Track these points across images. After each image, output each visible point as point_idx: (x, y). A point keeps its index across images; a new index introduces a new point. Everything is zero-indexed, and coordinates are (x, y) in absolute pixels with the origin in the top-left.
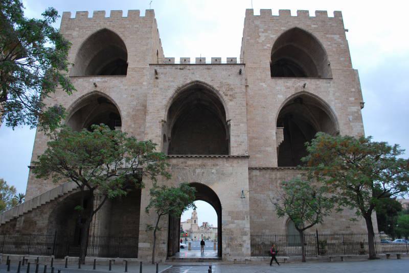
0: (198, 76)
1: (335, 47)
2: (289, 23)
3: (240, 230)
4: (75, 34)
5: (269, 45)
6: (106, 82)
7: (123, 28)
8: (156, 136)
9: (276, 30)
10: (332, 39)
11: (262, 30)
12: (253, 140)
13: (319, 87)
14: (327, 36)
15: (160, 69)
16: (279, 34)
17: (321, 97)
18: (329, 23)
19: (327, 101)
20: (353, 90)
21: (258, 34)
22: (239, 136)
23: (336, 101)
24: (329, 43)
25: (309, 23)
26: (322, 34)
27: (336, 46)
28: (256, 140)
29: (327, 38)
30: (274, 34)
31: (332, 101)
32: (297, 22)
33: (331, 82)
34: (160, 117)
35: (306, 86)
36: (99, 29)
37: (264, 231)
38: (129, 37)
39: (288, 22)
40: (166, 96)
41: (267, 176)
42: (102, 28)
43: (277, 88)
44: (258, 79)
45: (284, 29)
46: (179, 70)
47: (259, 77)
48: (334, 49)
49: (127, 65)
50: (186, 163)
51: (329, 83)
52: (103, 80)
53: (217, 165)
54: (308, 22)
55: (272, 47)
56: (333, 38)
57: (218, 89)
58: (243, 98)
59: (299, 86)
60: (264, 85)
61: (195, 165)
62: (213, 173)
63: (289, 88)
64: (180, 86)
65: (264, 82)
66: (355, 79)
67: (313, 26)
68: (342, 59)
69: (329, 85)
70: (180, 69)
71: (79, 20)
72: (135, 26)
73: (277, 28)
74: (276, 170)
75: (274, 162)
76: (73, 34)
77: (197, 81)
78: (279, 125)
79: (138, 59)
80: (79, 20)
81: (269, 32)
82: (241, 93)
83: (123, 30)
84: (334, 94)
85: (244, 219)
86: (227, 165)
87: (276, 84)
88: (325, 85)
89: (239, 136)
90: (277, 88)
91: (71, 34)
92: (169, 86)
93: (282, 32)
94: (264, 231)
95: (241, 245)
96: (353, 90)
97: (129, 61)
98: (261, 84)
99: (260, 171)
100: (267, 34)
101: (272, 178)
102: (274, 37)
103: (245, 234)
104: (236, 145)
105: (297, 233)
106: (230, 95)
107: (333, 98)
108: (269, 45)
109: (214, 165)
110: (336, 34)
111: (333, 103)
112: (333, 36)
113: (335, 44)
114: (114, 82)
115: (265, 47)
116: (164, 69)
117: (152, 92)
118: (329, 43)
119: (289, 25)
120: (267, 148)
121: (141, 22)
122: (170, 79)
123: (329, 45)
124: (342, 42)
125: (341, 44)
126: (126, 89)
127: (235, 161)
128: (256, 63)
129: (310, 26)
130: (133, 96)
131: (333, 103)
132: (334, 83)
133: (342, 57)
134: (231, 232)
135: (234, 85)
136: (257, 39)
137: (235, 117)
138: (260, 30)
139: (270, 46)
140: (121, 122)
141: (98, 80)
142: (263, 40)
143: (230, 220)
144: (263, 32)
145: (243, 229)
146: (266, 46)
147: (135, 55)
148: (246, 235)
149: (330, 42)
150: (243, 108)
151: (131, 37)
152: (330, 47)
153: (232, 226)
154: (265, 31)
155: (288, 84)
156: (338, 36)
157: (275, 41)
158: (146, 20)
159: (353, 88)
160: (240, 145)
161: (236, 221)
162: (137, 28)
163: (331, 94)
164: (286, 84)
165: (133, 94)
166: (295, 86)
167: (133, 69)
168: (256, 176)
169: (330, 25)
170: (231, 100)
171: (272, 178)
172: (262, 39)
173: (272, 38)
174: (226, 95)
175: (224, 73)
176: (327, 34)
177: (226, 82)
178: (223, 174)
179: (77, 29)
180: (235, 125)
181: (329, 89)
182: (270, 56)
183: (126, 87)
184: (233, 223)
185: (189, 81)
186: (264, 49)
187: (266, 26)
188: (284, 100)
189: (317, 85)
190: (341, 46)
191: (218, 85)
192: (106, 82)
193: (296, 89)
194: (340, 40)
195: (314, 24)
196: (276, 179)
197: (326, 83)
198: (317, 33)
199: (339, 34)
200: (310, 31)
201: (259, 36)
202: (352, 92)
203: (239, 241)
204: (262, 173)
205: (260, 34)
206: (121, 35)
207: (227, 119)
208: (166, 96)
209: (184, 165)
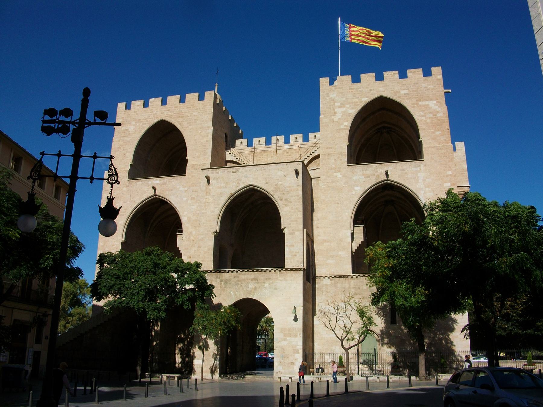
0: (251, 179)
1: (430, 118)
2: (372, 92)
3: (293, 347)
4: (131, 128)
5: (346, 124)
6: (165, 184)
7: (182, 117)
8: (209, 250)
9: (354, 102)
10: (427, 106)
11: (339, 104)
12: (325, 244)
13: (406, 173)
14: (420, 103)
15: (213, 173)
16: (359, 108)
17: (407, 185)
18: (424, 85)
19: (414, 190)
20: (450, 173)
21: (334, 110)
22: (293, 246)
23: (427, 189)
24: (422, 113)
25: (397, 88)
26: (414, 101)
27: (431, 115)
28: (328, 243)
29: (421, 105)
30: (352, 109)
31: (421, 189)
32: (381, 89)
33: (422, 165)
34: (212, 228)
35: (389, 173)
36: (156, 121)
37: (334, 348)
38: (188, 127)
39: (371, 90)
40: (218, 205)
41: (339, 285)
42: (159, 119)
43: (354, 178)
44: (332, 169)
45: (366, 100)
46: (232, 174)
47: (333, 166)
48: (428, 121)
49: (186, 161)
50: (238, 277)
51: (419, 166)
52: (162, 182)
53: (270, 279)
54: (396, 88)
55: (350, 125)
56: (428, 105)
57: (271, 193)
58: (299, 202)
59: (381, 173)
60: (339, 175)
61: (247, 279)
62: (266, 288)
63: (367, 177)
64: (233, 192)
65: (339, 172)
66: (453, 158)
67: (403, 92)
68: (438, 133)
69: (418, 169)
70: (233, 172)
71: (135, 112)
72: (194, 114)
73: (357, 100)
74: (349, 278)
75: (348, 269)
76: (130, 130)
77: (251, 185)
78: (356, 221)
79: (197, 154)
80: (135, 112)
81: (348, 106)
82: (298, 196)
83: (181, 119)
84: (424, 180)
85: (296, 336)
86: (281, 278)
87: (353, 173)
88: (414, 169)
89: (293, 246)
90: (354, 178)
91: (127, 130)
92: (221, 193)
93: (363, 104)
94: (334, 348)
95: (293, 363)
96: (450, 173)
97: (188, 157)
98: (335, 174)
99: (331, 280)
100: (344, 109)
101: (345, 288)
102: (353, 111)
103: (297, 352)
104: (290, 256)
105: (344, 351)
106: (286, 200)
107: (423, 186)
108: (346, 124)
109: (266, 279)
110: (431, 100)
111: (423, 192)
112: (427, 103)
113: (430, 113)
114: (173, 183)
115: (342, 127)
116: (218, 173)
117: (204, 200)
118: (422, 113)
119: (372, 94)
120: (340, 253)
121: (200, 109)
122: (223, 185)
123: (422, 116)
124: (440, 109)
125: (438, 112)
126: (185, 191)
127: (289, 273)
128: (330, 148)
129: (399, 92)
130: (194, 198)
131: (423, 192)
132: (425, 165)
133: (439, 130)
134: (283, 349)
135: (290, 187)
136: (333, 117)
137: (290, 224)
138: (336, 104)
139: (347, 124)
140: (181, 228)
141: (156, 181)
142: (340, 117)
143: (282, 337)
144: (339, 107)
145: (296, 346)
146: (342, 124)
147: (195, 149)
148: (298, 353)
149: (423, 111)
150: (299, 213)
151: (190, 127)
152: (423, 118)
153: (285, 343)
154: (342, 105)
155: (368, 172)
156: (435, 102)
157: (354, 117)
158: (206, 106)
159: (449, 170)
160: (295, 255)
161: (288, 338)
162: (196, 116)
163: (420, 181)
164: (364, 172)
165: (194, 196)
166: (376, 174)
167: (193, 166)
168: (326, 285)
169: (426, 87)
170: (286, 205)
171: (345, 288)
172: (339, 115)
173: (351, 113)
174: (281, 200)
175: (279, 173)
176: (420, 101)
177: (281, 184)
178: (275, 289)
179: (133, 123)
180: (290, 234)
181: (419, 175)
182: (346, 137)
183: (186, 189)
184: (285, 340)
185: (241, 187)
186: (340, 129)
187: (344, 99)
188: (362, 193)
189: (404, 170)
190: (438, 115)
191: (272, 189)
192: (165, 184)
193: (378, 176)
194: (437, 108)
195: (404, 89)
196: (349, 288)
197: (415, 166)
198: (408, 101)
199: (436, 99)
200: (398, 100)
201: (335, 113)
202: (448, 176)
203: (291, 359)
204: (333, 282)
205: (336, 110)
206: (179, 127)
207: (282, 227)
208: (218, 205)
209: (236, 279)
